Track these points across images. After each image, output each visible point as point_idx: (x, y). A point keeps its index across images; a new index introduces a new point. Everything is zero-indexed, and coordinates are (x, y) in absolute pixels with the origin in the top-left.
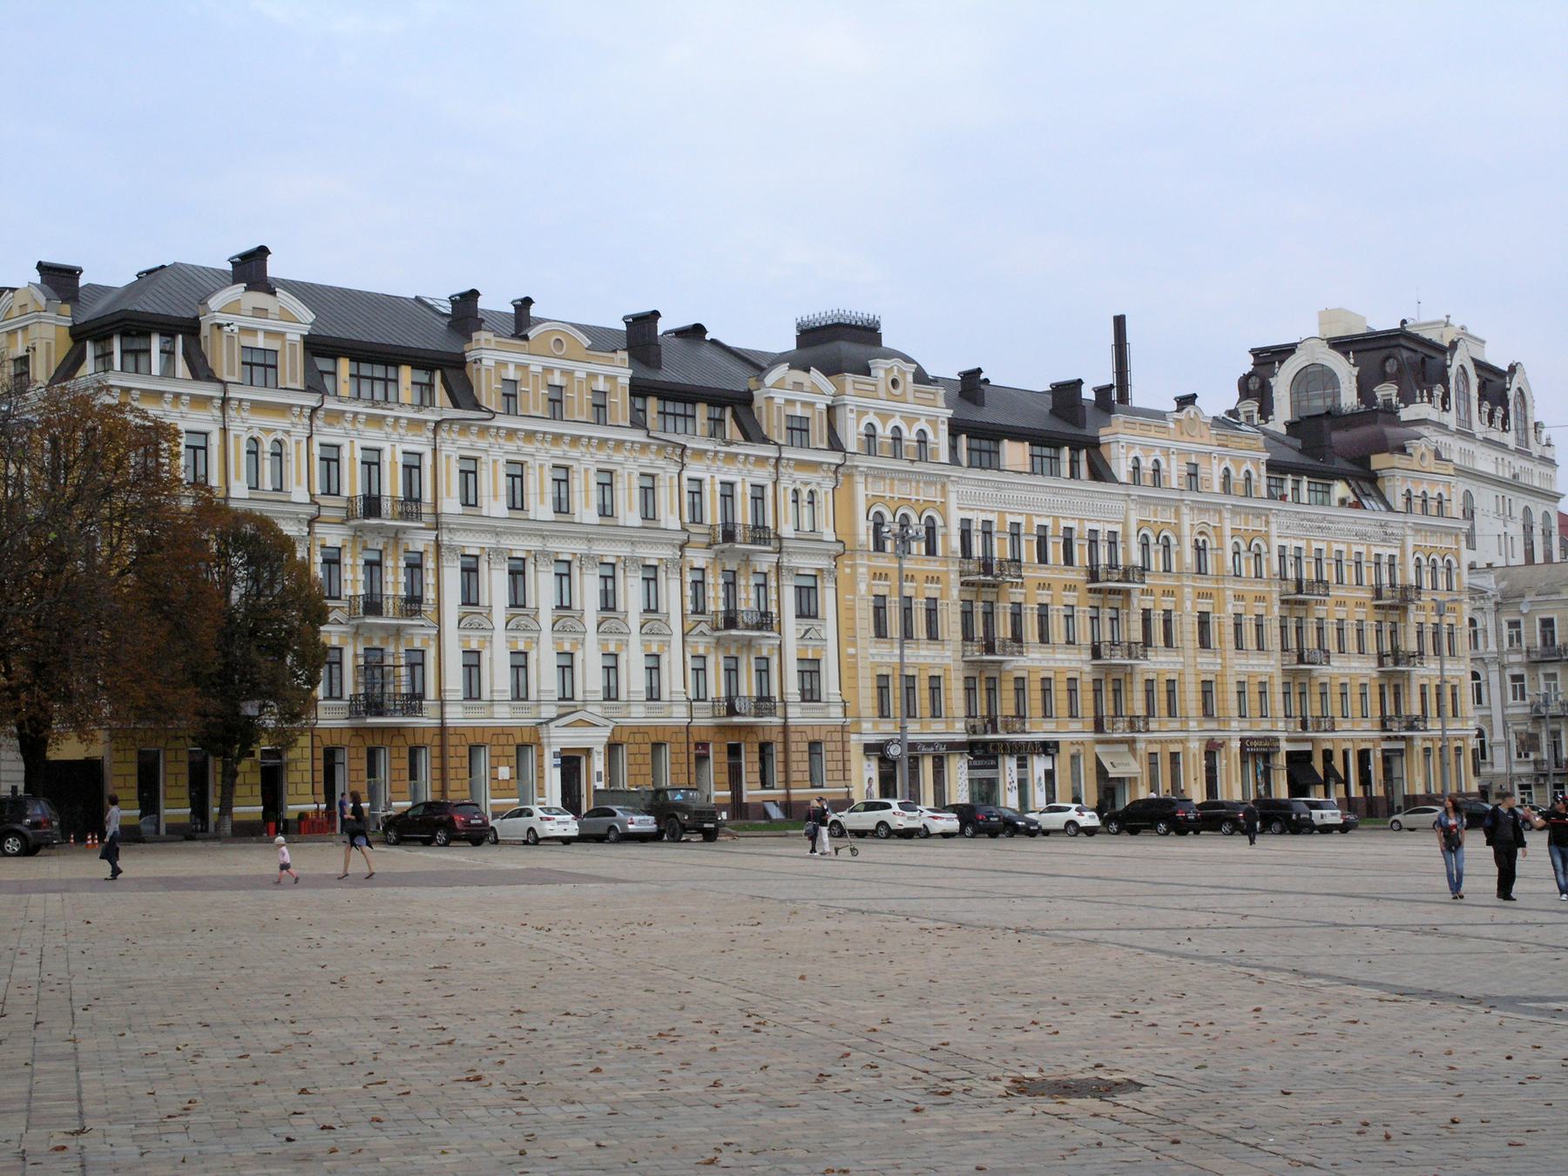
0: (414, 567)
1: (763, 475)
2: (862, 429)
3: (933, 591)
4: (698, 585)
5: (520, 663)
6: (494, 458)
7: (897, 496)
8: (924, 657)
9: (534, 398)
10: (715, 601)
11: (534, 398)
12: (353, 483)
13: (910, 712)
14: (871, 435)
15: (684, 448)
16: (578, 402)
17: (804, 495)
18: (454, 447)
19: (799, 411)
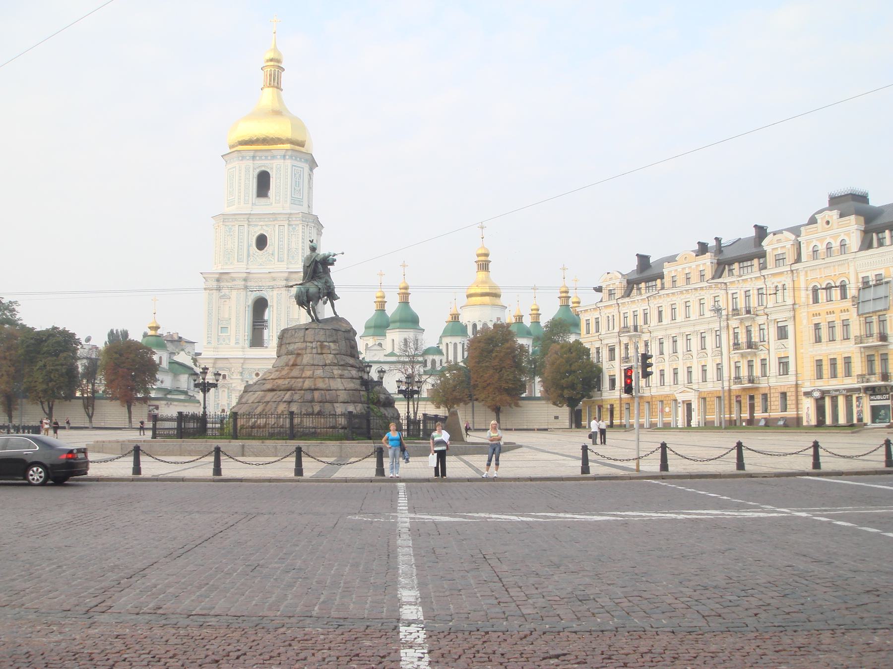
0: (646, 345)
1: (760, 284)
2: (811, 249)
3: (845, 316)
4: (736, 335)
5: (719, 368)
6: (693, 299)
7: (837, 273)
8: (841, 349)
9: (681, 281)
10: (742, 339)
11: (681, 281)
12: (630, 323)
13: (834, 375)
14: (815, 251)
15: (725, 284)
16: (695, 277)
17: (780, 286)
18: (654, 304)
19: (779, 251)
